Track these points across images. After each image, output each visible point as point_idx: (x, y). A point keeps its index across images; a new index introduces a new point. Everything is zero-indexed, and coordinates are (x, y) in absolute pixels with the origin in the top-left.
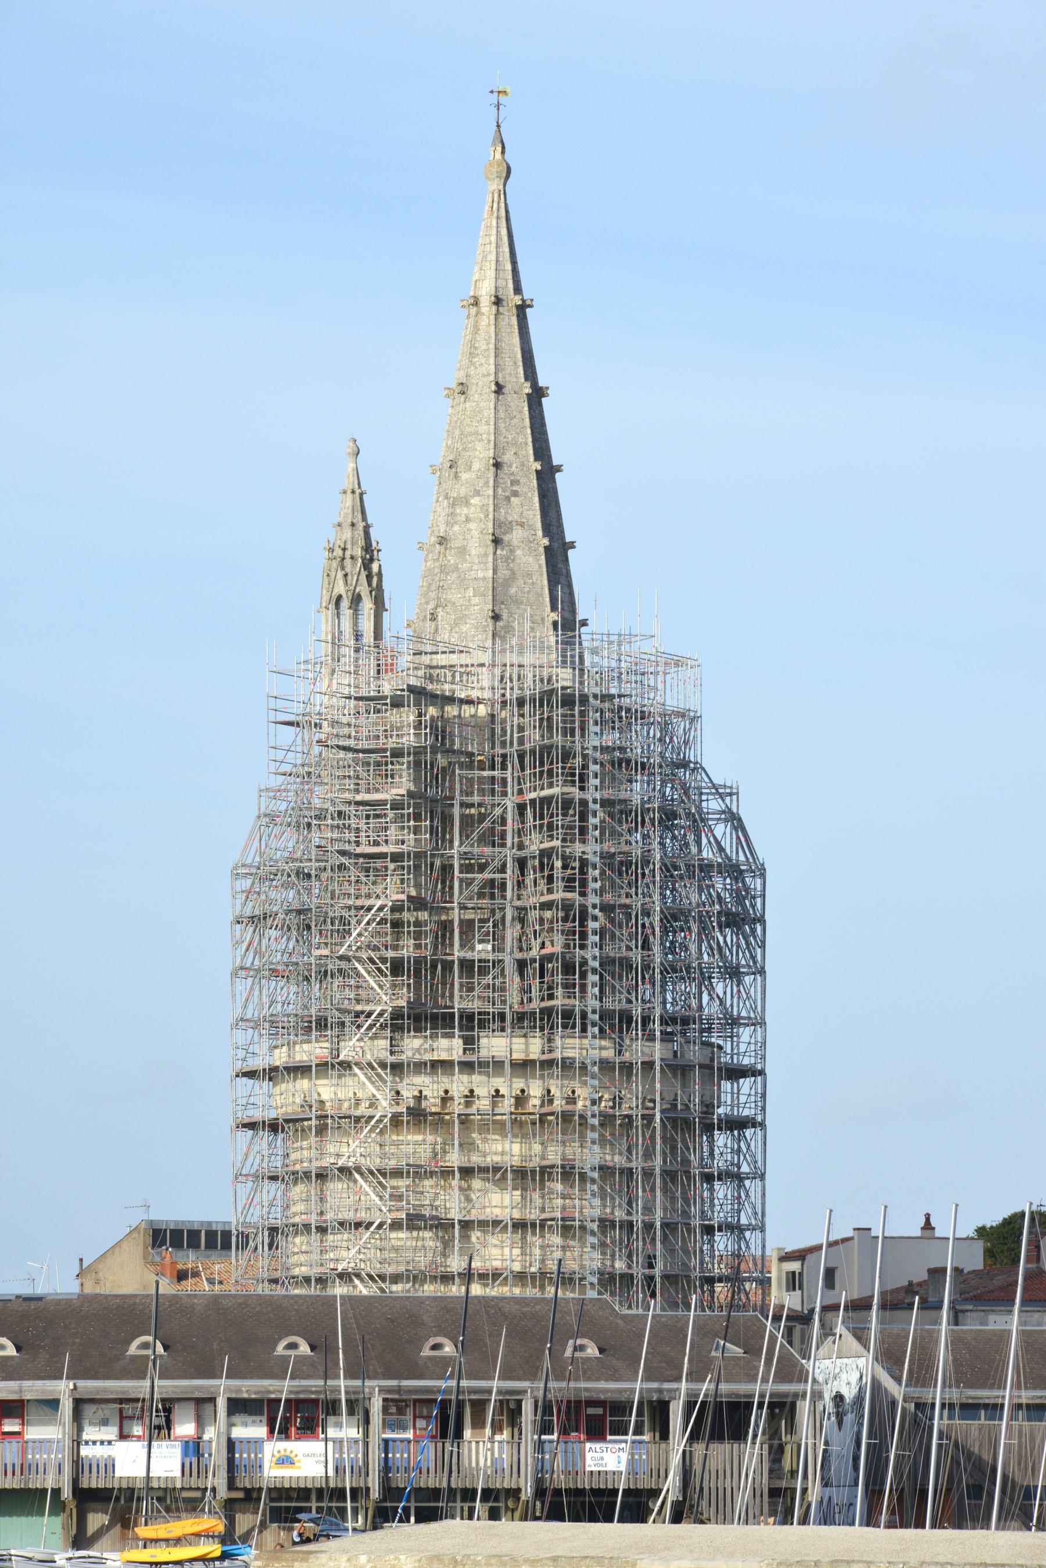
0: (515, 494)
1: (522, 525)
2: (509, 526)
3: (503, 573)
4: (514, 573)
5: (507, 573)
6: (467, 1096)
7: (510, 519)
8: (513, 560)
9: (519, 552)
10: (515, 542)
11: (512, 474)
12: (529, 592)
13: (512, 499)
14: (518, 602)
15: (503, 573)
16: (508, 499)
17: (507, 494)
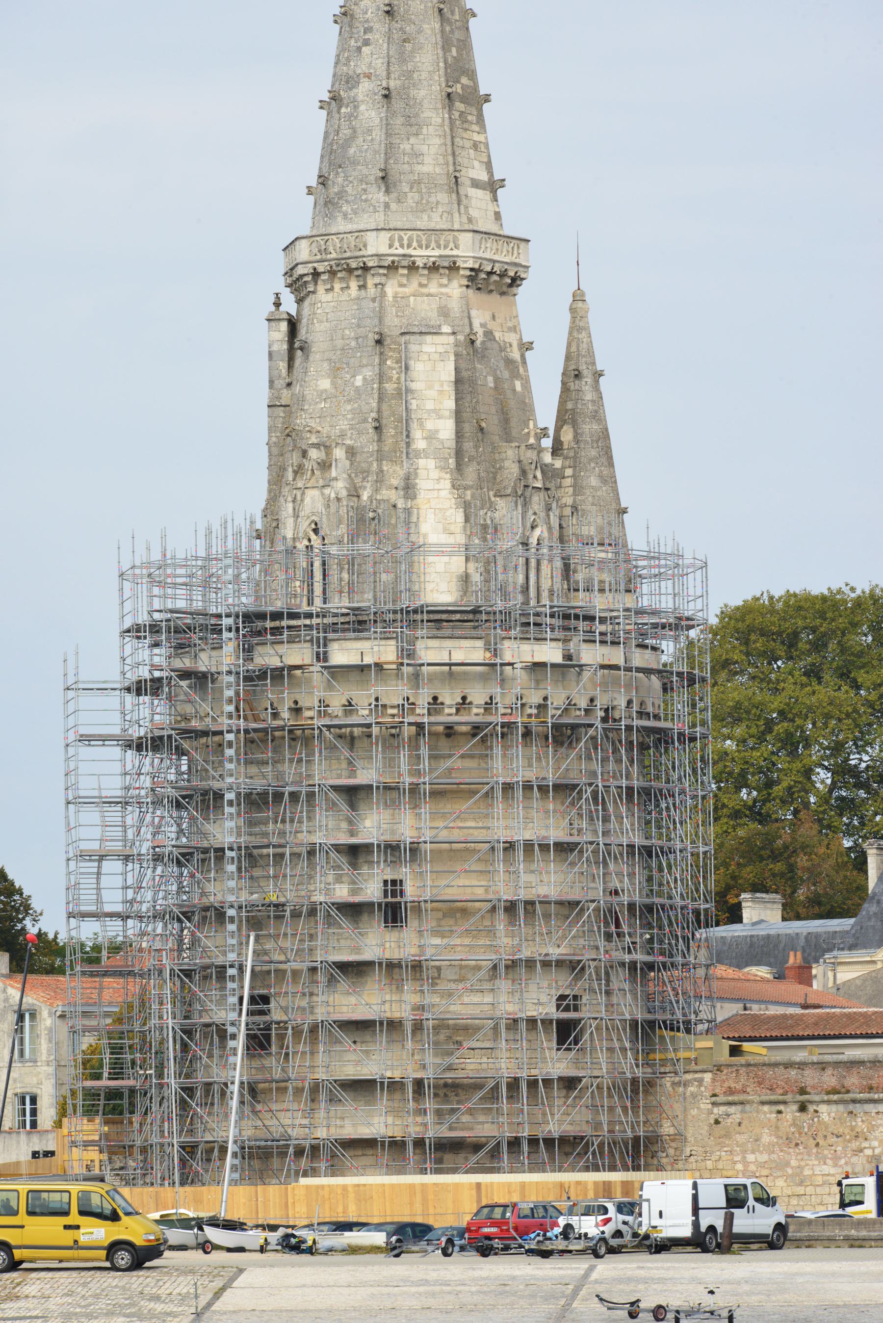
0: (367, 43)
1: (368, 76)
2: (351, 81)
3: (346, 132)
4: (355, 132)
5: (348, 132)
6: (344, 706)
7: (358, 72)
8: (356, 117)
9: (362, 108)
10: (360, 97)
11: (367, 21)
12: (366, 151)
13: (364, 49)
14: (354, 163)
15: (346, 132)
16: (359, 49)
17: (359, 44)
